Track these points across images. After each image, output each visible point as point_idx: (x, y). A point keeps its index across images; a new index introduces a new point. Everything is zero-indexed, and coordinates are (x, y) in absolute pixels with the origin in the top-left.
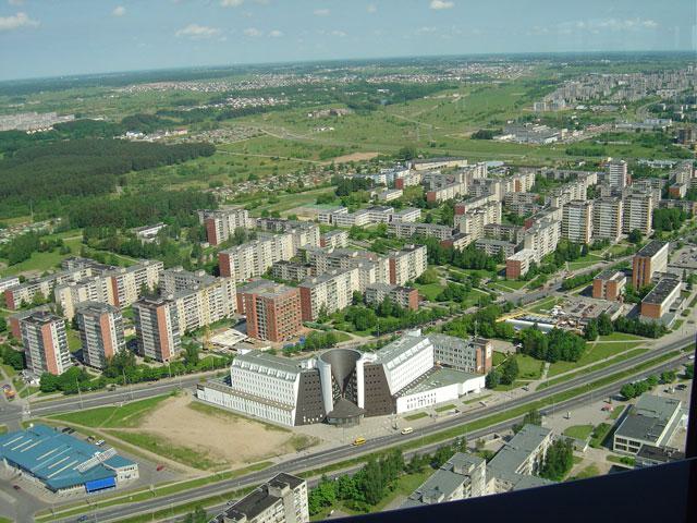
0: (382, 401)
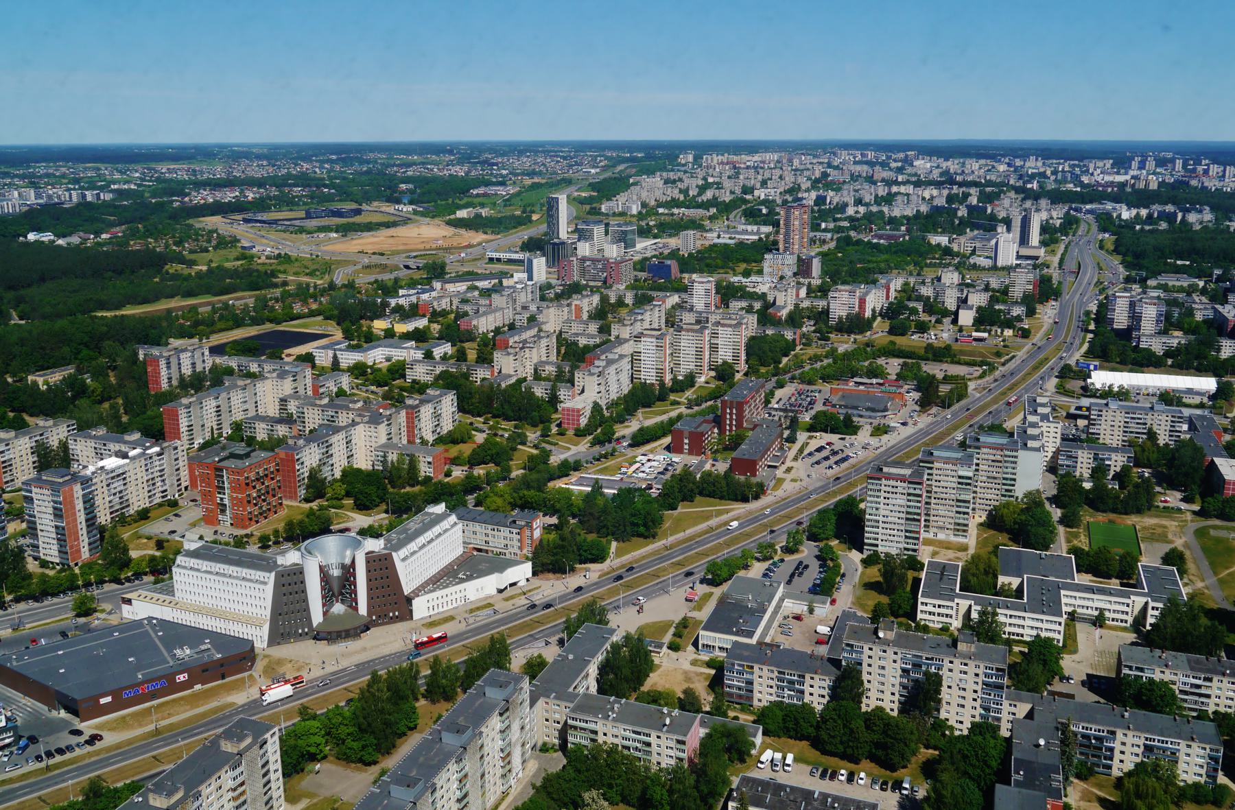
0: (392, 602)
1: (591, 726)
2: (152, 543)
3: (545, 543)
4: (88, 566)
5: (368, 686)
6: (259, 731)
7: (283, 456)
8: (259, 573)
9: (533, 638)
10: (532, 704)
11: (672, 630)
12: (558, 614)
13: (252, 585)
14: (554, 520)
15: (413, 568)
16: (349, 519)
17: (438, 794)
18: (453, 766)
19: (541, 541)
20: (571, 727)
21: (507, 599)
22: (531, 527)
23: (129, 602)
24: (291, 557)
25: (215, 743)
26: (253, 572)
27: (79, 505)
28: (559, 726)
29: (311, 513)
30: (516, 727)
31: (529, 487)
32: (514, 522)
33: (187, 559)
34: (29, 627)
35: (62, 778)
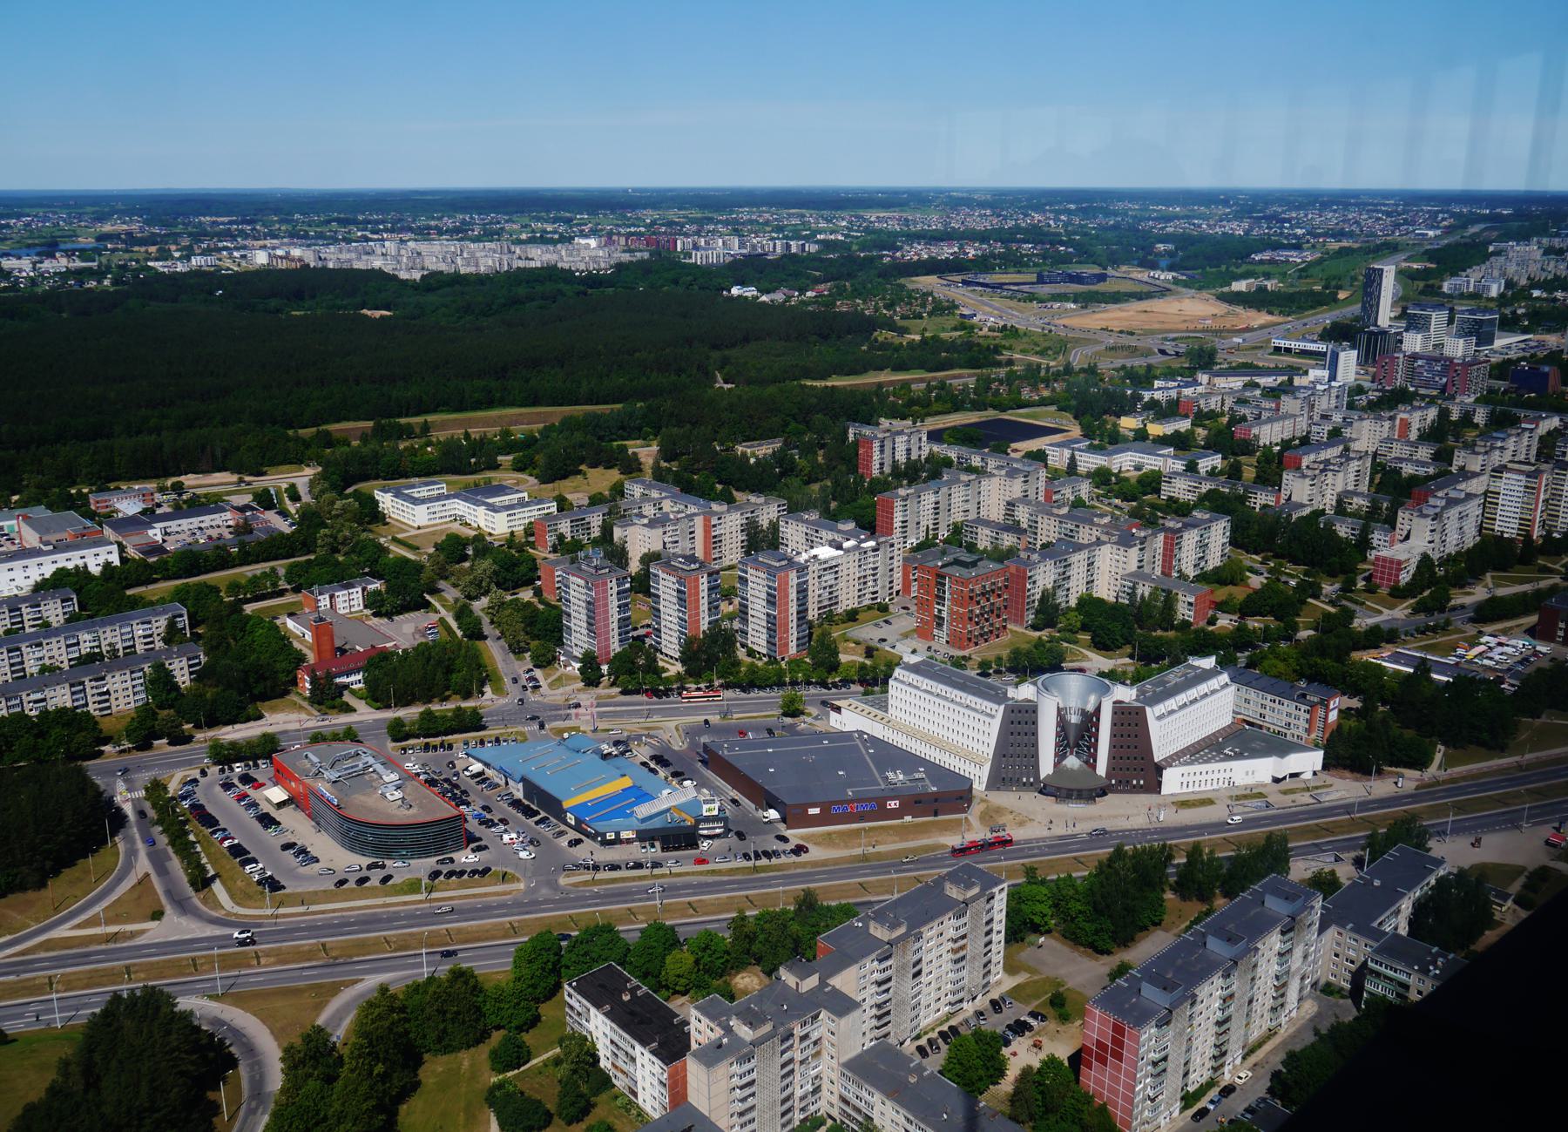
0: (1138, 768)
1: (1403, 977)
2: (861, 649)
3: (1346, 728)
4: (795, 663)
5: (1110, 860)
6: (990, 881)
7: (1013, 570)
8: (986, 703)
9: (1318, 849)
10: (1321, 931)
11: (1522, 880)
12: (1354, 825)
13: (977, 716)
14: (1355, 703)
15: (1174, 725)
16: (1085, 658)
17: (1198, 1008)
18: (1218, 981)
19: (1340, 726)
20: (1372, 972)
21: (1285, 793)
22: (1327, 706)
23: (838, 709)
24: (1025, 692)
25: (939, 882)
26: (979, 701)
27: (793, 595)
28: (1353, 967)
29: (1039, 643)
30: (1298, 952)
31: (1323, 655)
32: (1304, 696)
33: (906, 673)
34: (737, 717)
35: (764, 883)
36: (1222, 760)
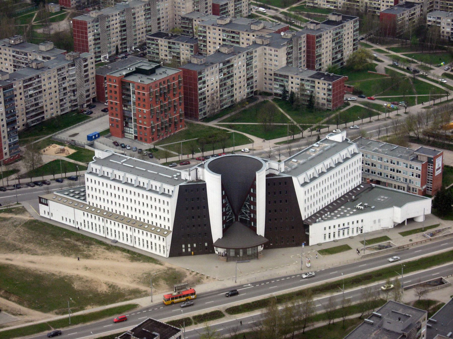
36: (355, 214)
